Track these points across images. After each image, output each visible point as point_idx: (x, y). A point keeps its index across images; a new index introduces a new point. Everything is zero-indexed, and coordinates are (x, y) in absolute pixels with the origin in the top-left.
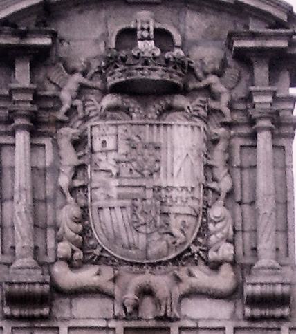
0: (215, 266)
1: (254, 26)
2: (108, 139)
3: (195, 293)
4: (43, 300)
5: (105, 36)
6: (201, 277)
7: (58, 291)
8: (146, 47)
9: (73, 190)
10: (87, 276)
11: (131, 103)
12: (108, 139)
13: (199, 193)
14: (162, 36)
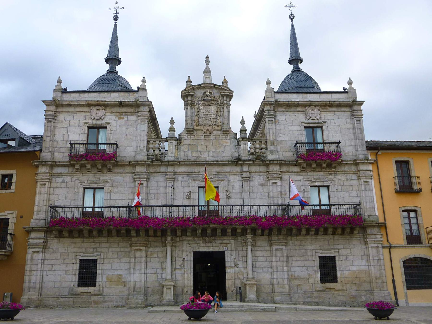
0: (218, 126)
1: (224, 91)
2: (202, 107)
3: (215, 130)
4: (192, 131)
5: (202, 93)
6: (216, 128)
7: (194, 129)
8: (208, 94)
9: (197, 115)
10: (199, 127)
11: (206, 102)
12: (202, 107)
13: (216, 115)
14: (210, 93)
